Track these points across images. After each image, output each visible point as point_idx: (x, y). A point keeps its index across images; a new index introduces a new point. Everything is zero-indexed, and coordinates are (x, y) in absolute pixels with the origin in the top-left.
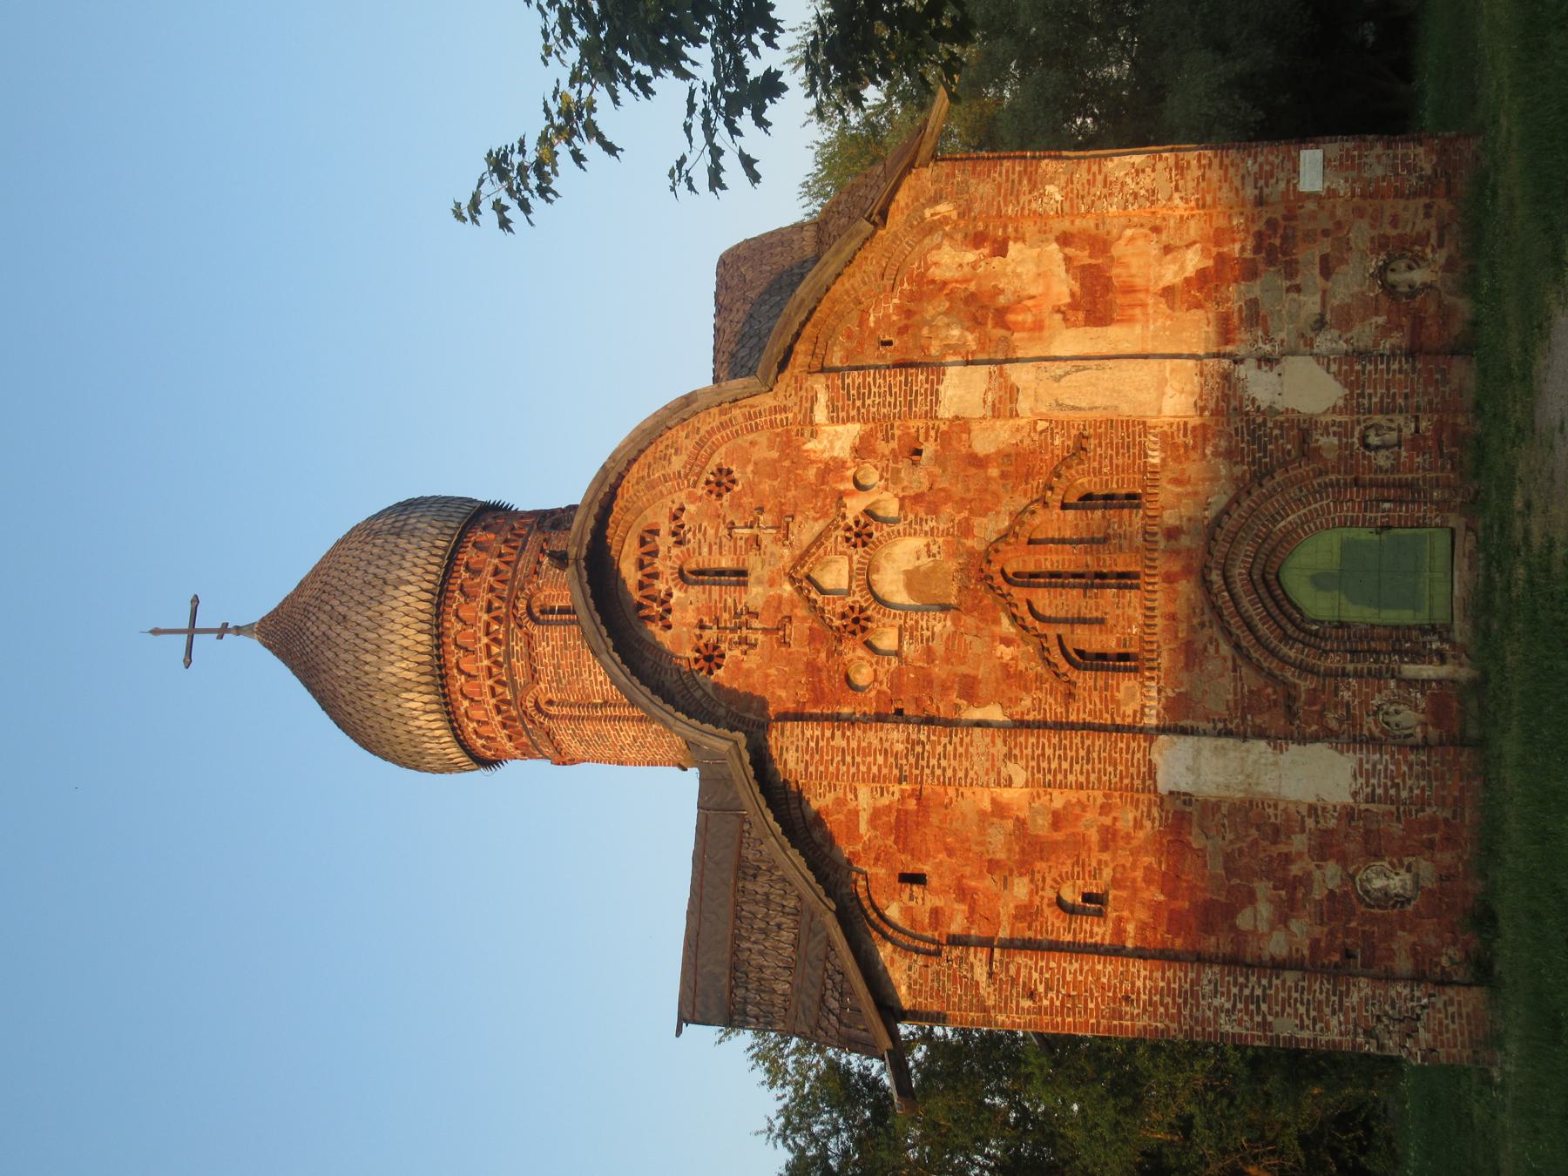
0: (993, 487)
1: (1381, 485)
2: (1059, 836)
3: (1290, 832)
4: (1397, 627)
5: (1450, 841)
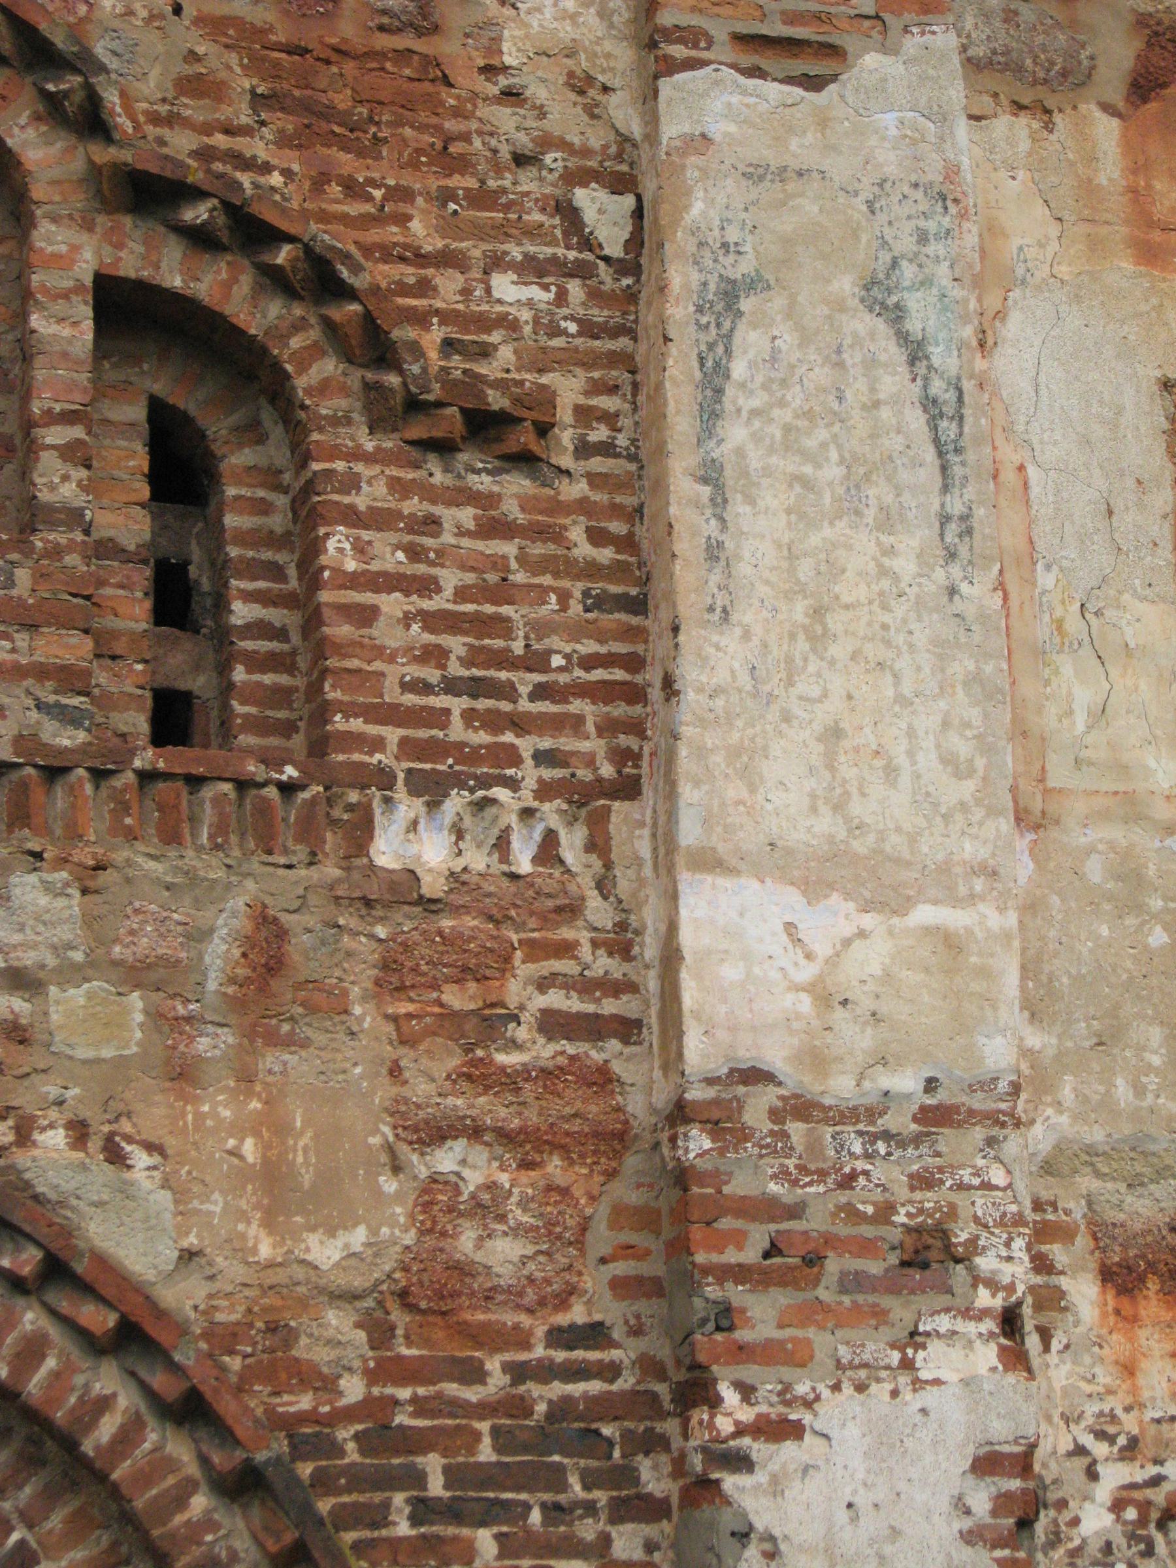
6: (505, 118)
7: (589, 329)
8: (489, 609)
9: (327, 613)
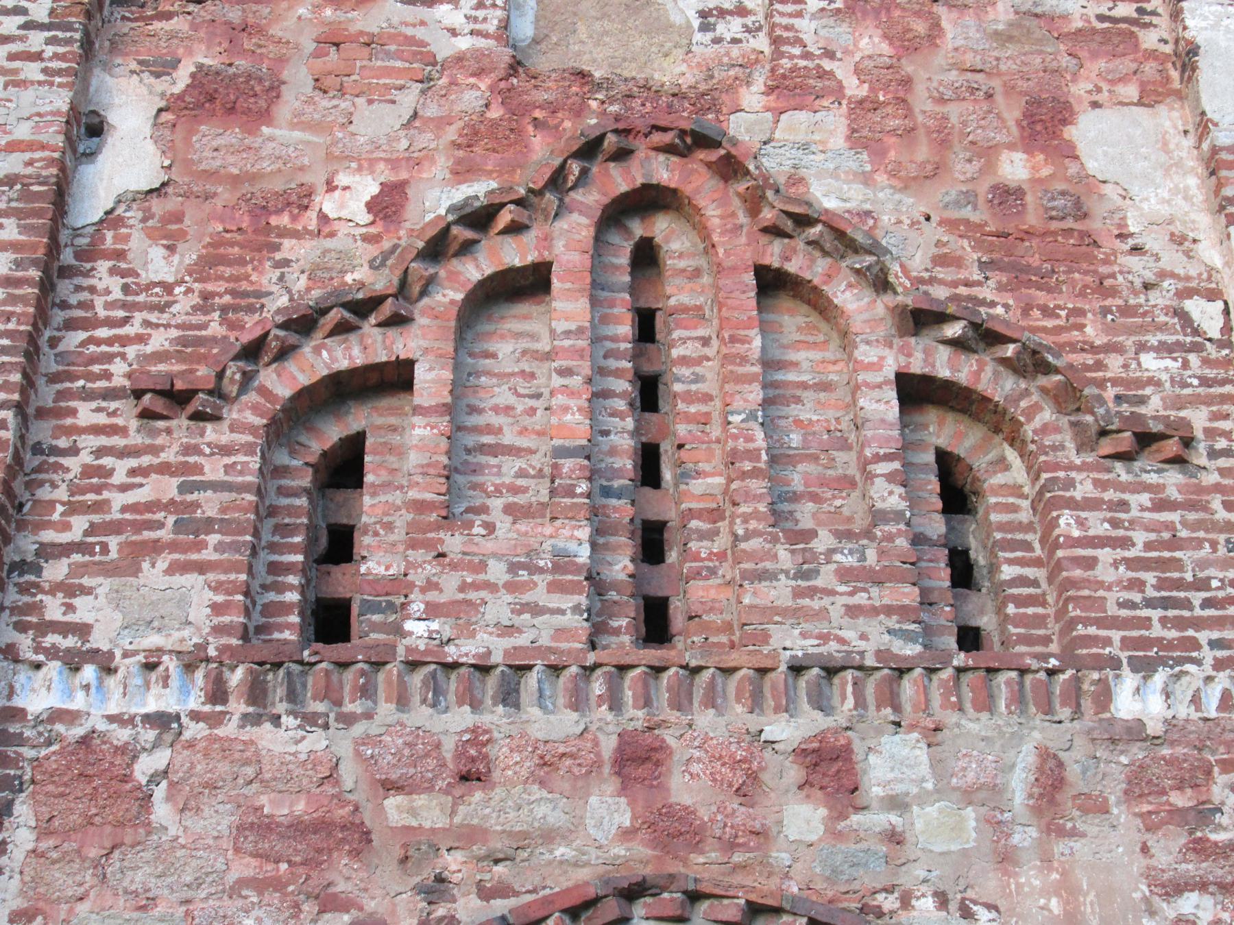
0: (962, 167)
6: (1134, 262)
7: (1205, 382)
8: (1166, 554)
9: (1065, 563)
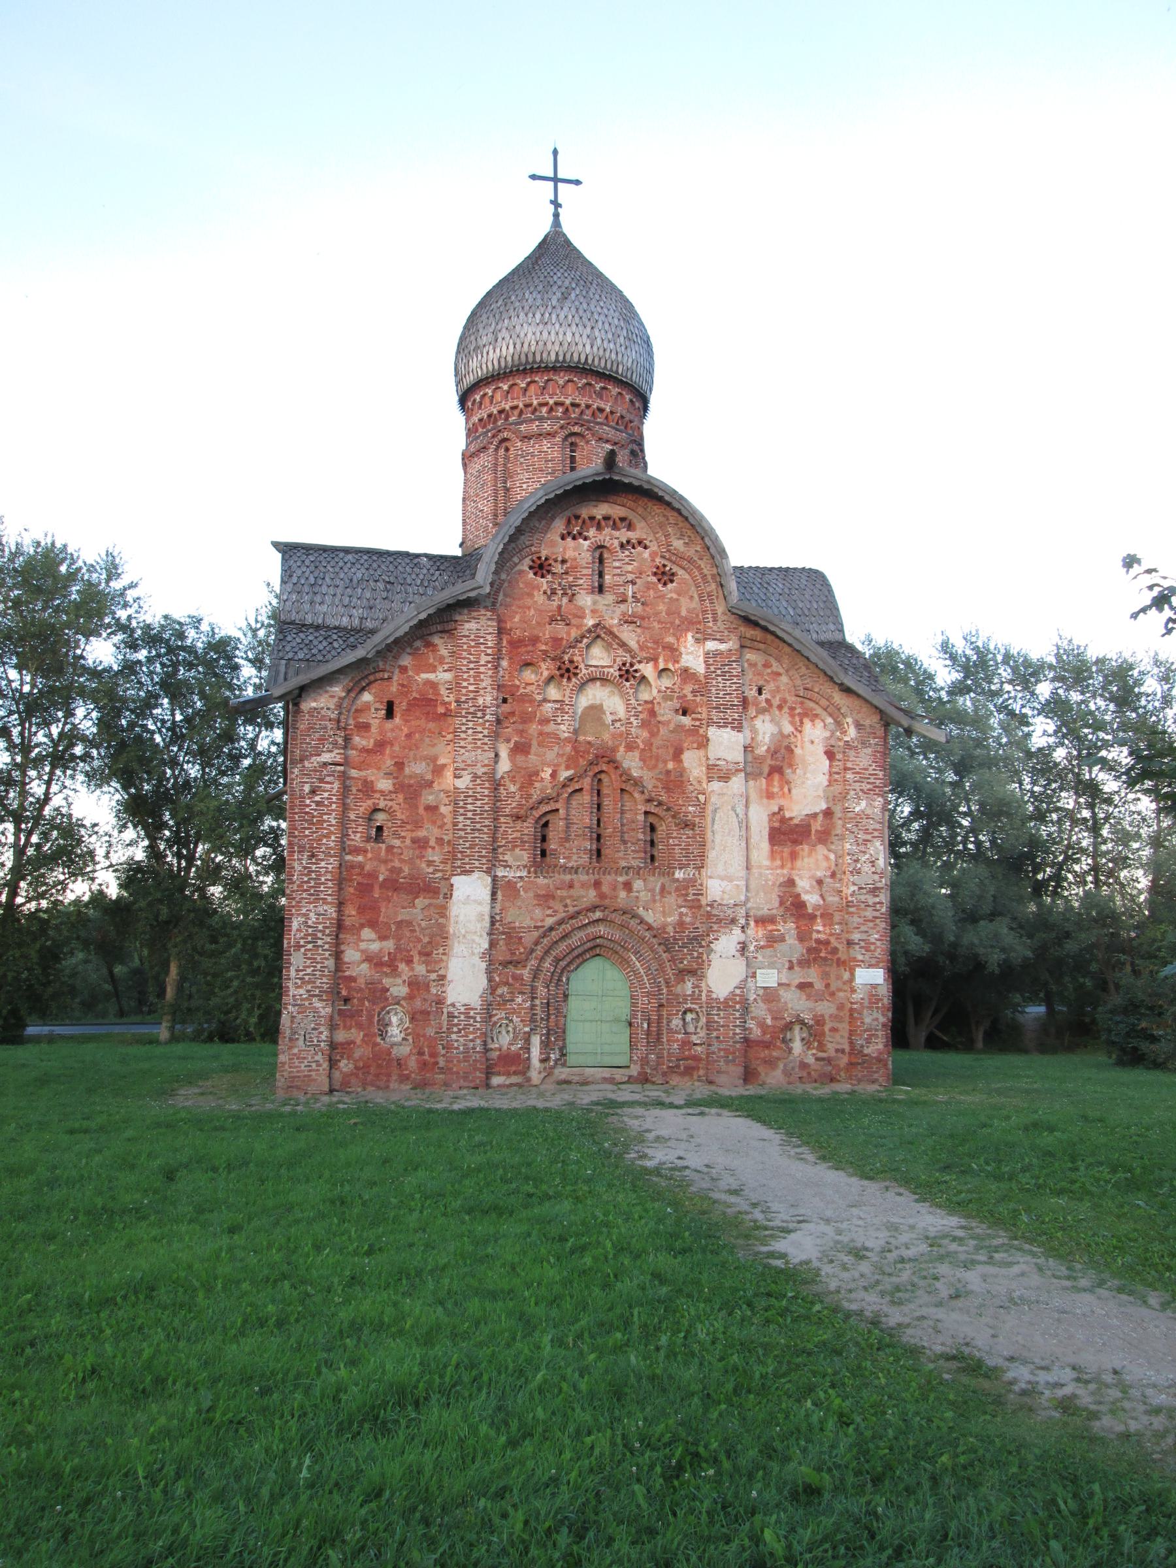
0: (661, 765)
1: (659, 1021)
2: (421, 811)
3: (427, 963)
4: (564, 1032)
5: (424, 1065)
